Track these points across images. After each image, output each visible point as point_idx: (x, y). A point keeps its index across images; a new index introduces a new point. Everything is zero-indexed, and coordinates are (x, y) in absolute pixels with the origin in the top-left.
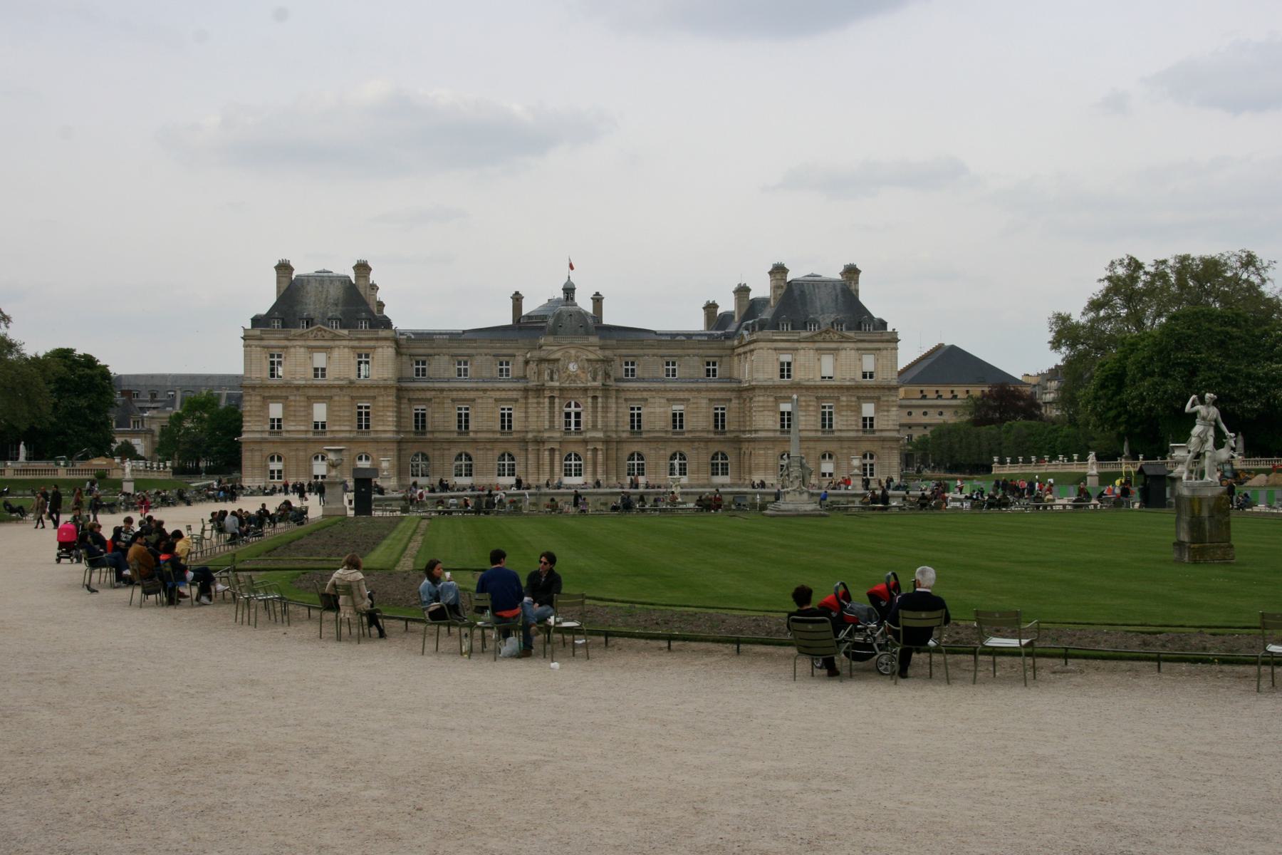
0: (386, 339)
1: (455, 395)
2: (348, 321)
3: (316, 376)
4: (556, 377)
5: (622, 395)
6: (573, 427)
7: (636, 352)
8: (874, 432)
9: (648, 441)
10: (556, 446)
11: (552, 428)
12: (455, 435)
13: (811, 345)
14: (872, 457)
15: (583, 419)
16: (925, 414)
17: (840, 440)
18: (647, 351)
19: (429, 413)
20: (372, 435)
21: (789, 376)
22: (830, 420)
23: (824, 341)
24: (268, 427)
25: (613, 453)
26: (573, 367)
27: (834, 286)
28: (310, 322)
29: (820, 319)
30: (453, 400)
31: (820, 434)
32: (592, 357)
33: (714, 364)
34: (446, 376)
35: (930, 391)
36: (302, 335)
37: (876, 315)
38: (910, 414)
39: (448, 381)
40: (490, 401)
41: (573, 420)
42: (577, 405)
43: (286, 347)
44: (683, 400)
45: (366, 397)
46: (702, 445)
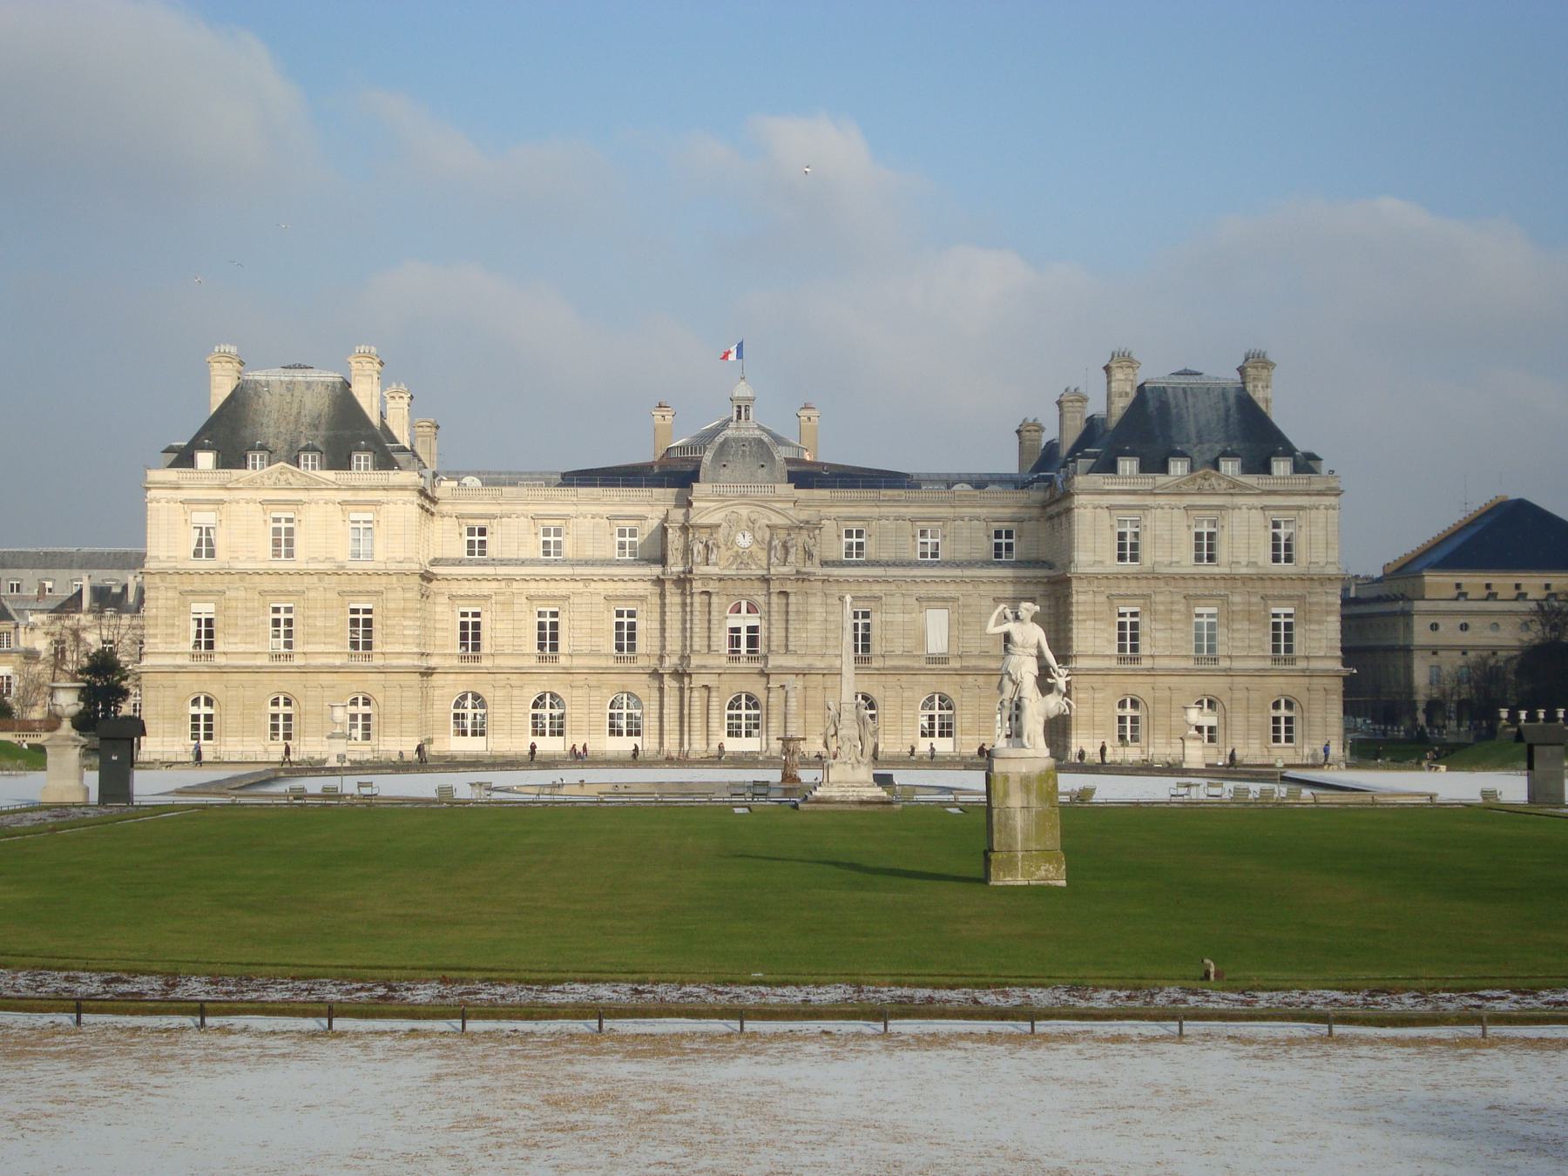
0: (403, 488)
1: (533, 588)
2: (339, 459)
3: (276, 554)
4: (713, 558)
6: (744, 648)
7: (863, 511)
8: (1293, 661)
9: (882, 672)
13: (1174, 500)
14: (1289, 705)
15: (762, 634)
16: (1464, 627)
17: (1228, 673)
19: (485, 621)
20: (377, 661)
21: (1134, 558)
22: (1211, 638)
23: (1200, 492)
24: (189, 646)
27: (1224, 394)
28: (272, 456)
29: (1195, 453)
31: (1191, 664)
32: (777, 520)
33: (1009, 534)
34: (523, 555)
35: (1474, 581)
36: (252, 480)
37: (1301, 445)
38: (1434, 627)
39: (523, 563)
41: (744, 635)
42: (752, 609)
43: (222, 502)
44: (944, 599)
45: (368, 593)
46: (981, 679)
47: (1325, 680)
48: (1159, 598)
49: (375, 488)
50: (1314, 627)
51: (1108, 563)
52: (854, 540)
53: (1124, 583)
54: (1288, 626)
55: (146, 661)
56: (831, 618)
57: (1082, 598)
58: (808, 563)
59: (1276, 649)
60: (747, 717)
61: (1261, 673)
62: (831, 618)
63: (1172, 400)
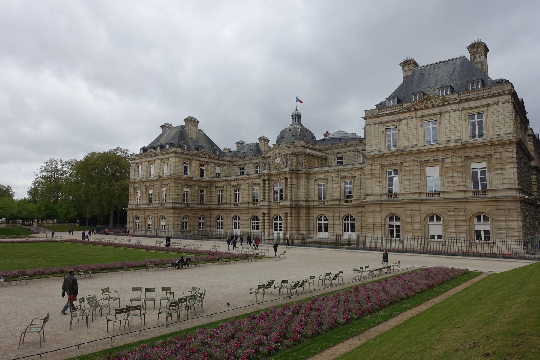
0: (171, 153)
1: (234, 183)
5: (313, 177)
7: (343, 150)
8: (485, 192)
9: (329, 207)
10: (266, 211)
11: (264, 199)
12: (233, 206)
13: (413, 114)
17: (446, 201)
18: (349, 149)
23: (426, 107)
25: (303, 216)
26: (278, 161)
30: (233, 186)
32: (288, 152)
36: (145, 155)
40: (247, 185)
42: (280, 185)
43: (142, 162)
47: (508, 204)
48: (406, 164)
49: (167, 154)
50: (500, 172)
51: (382, 149)
52: (340, 160)
53: (389, 159)
54: (483, 173)
55: (130, 207)
56: (312, 187)
57: (369, 167)
58: (300, 167)
59: (476, 186)
60: (280, 223)
61: (465, 201)
62: (312, 187)
63: (427, 73)
